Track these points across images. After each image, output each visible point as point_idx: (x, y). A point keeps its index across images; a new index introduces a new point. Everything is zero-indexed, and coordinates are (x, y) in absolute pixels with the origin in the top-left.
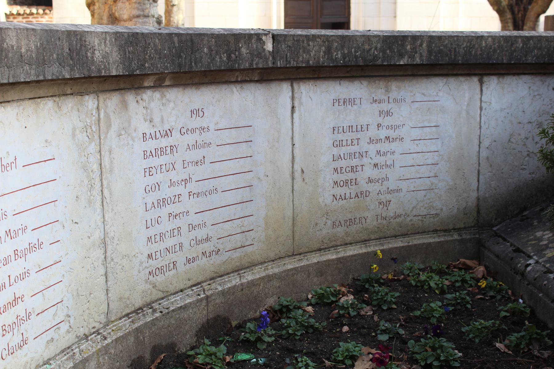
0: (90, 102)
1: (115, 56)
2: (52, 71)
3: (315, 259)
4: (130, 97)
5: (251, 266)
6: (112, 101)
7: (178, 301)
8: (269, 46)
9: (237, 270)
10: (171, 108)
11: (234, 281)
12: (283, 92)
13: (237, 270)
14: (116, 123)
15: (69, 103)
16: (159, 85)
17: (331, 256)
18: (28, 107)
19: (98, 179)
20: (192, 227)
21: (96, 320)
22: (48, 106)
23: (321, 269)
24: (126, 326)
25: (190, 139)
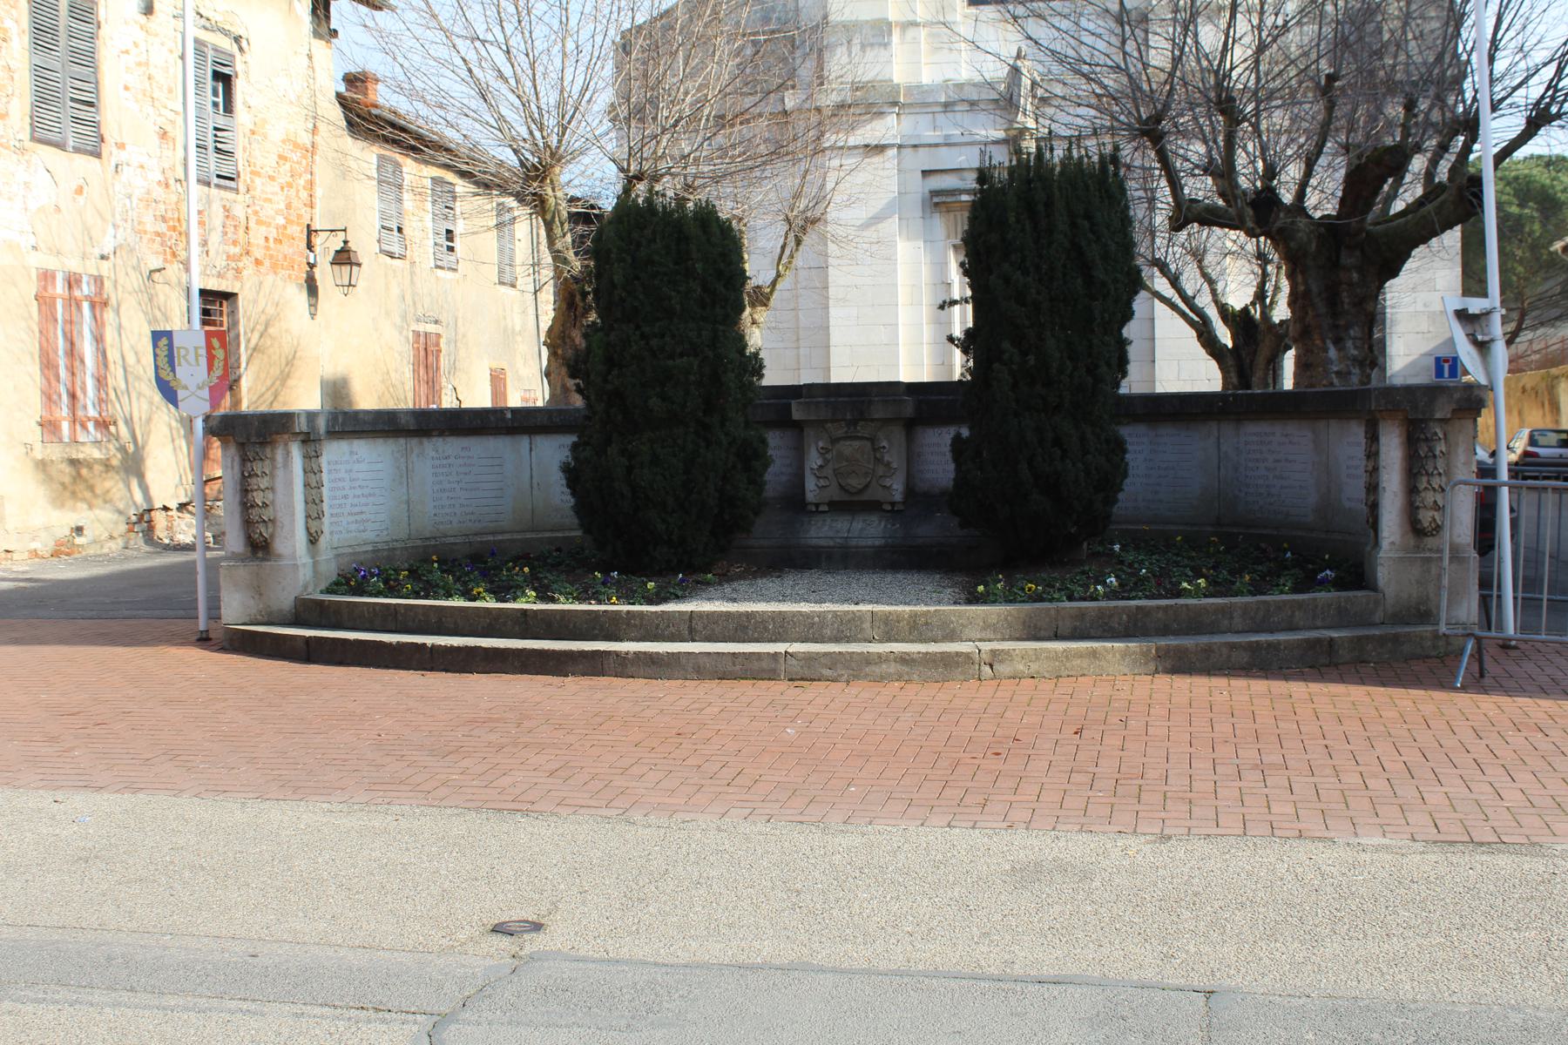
0: (402, 441)
1: (412, 421)
2: (380, 427)
3: (548, 535)
4: (425, 440)
5: (502, 533)
6: (414, 441)
7: (452, 540)
8: (509, 416)
9: (493, 533)
10: (452, 446)
11: (491, 538)
12: (524, 441)
13: (493, 533)
14: (416, 451)
15: (391, 441)
16: (441, 434)
17: (560, 535)
18: (371, 441)
19: (405, 475)
20: (462, 505)
21: (403, 535)
22: (380, 441)
23: (551, 541)
24: (419, 543)
25: (461, 461)
